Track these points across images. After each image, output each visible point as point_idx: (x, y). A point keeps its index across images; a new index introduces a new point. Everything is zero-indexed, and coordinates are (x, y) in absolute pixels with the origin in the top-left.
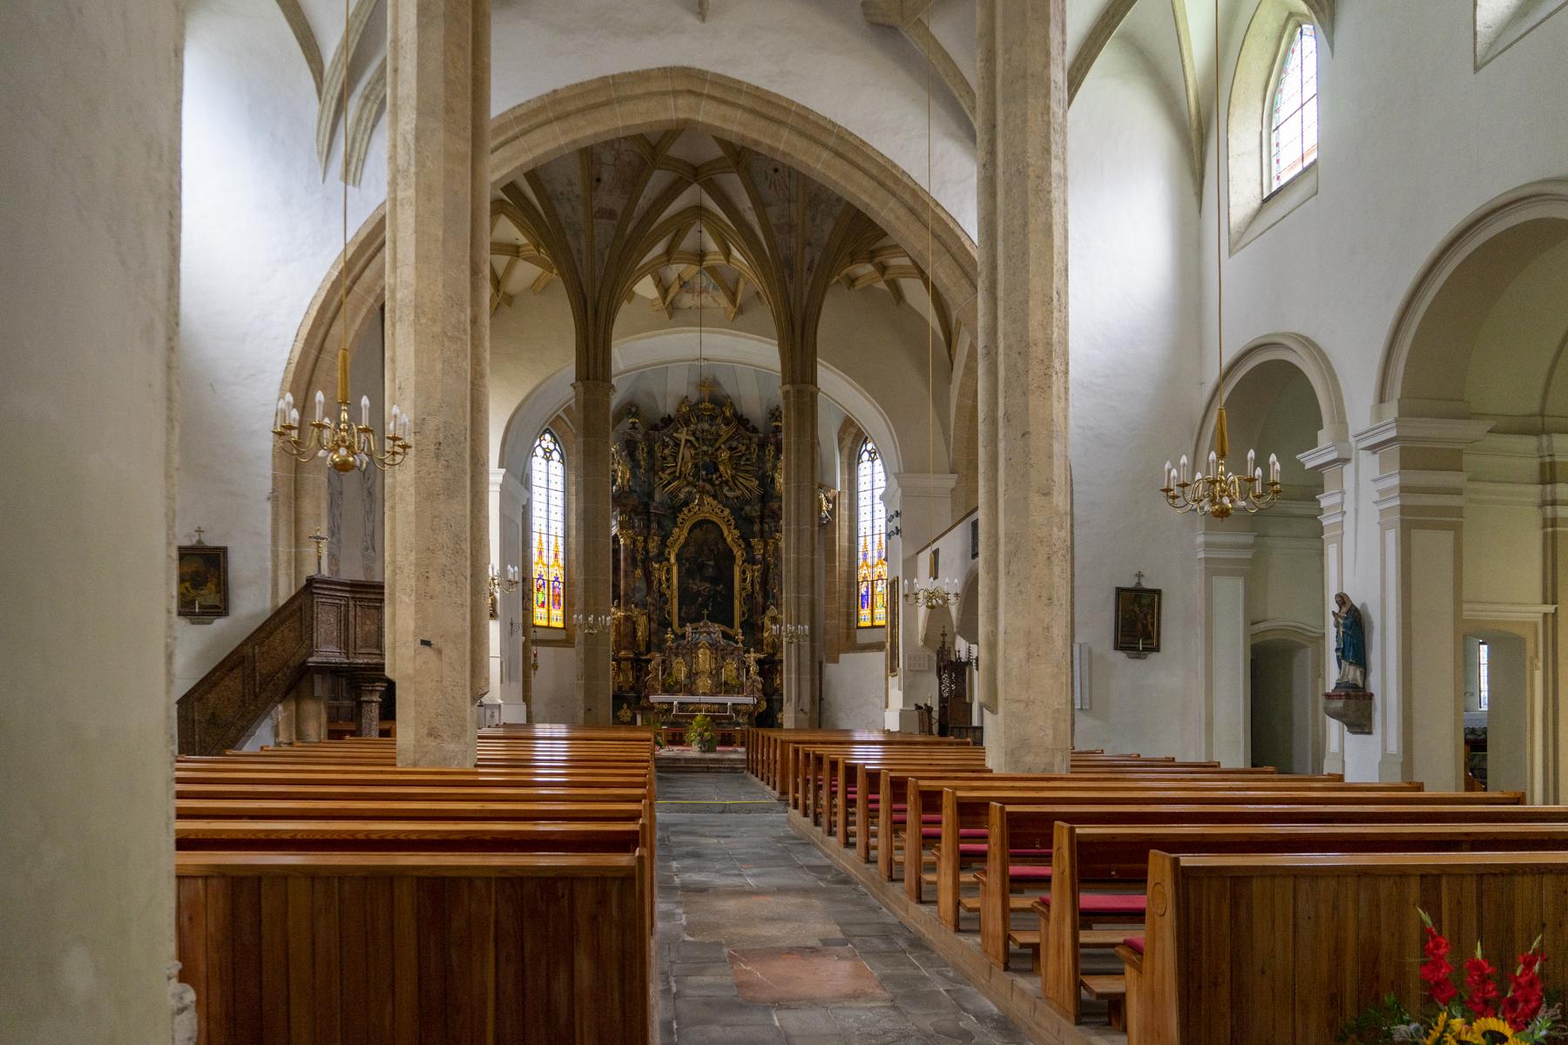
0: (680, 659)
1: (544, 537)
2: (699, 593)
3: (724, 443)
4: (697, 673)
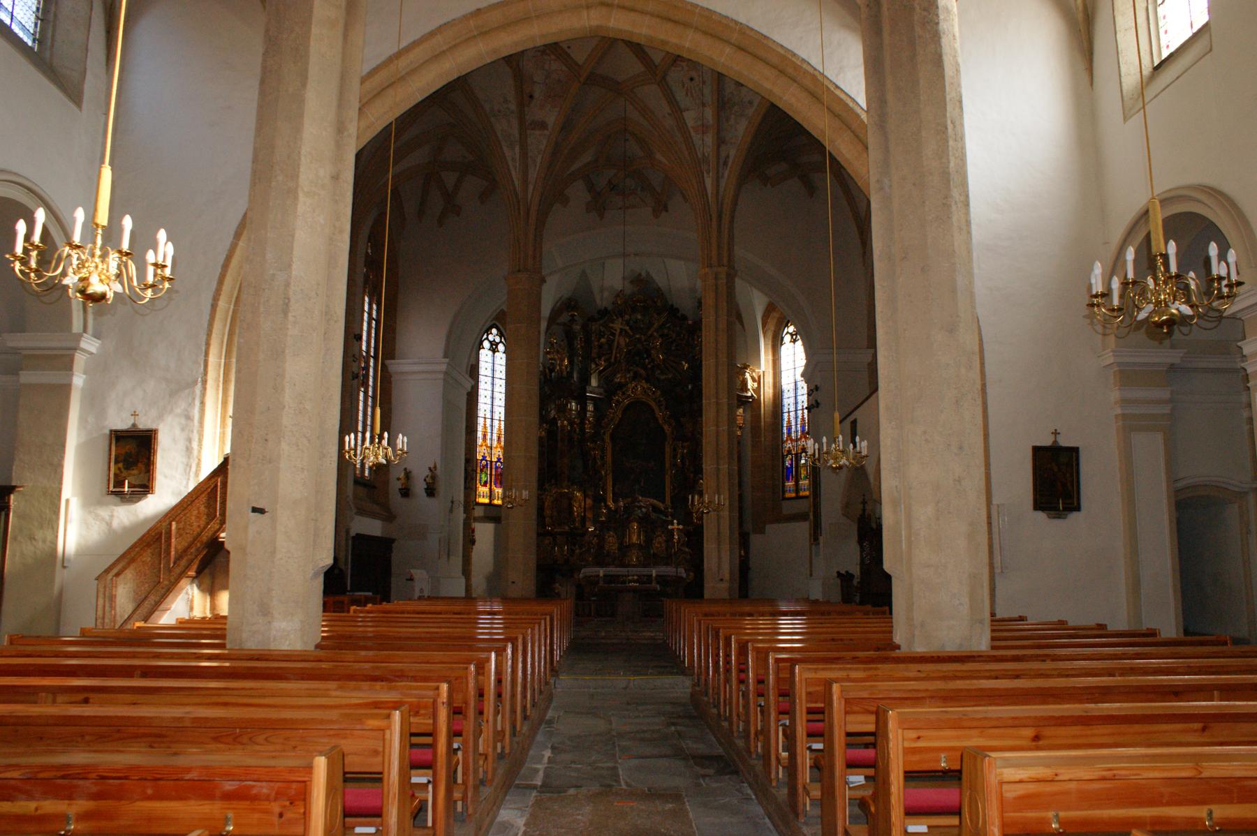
1: (488, 422)
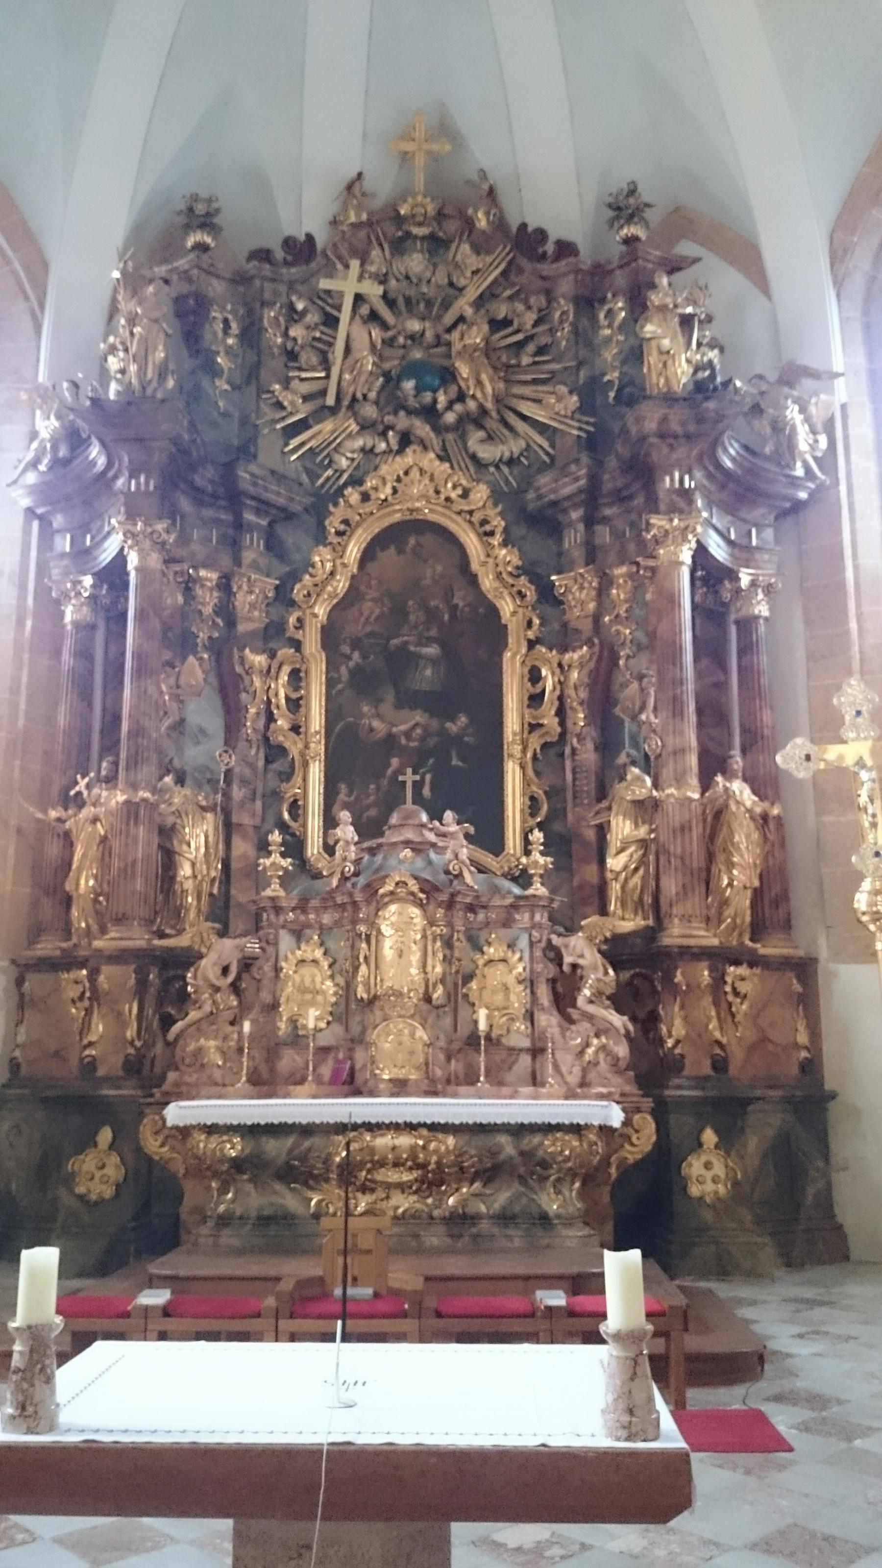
2: (390, 742)
3: (480, 302)
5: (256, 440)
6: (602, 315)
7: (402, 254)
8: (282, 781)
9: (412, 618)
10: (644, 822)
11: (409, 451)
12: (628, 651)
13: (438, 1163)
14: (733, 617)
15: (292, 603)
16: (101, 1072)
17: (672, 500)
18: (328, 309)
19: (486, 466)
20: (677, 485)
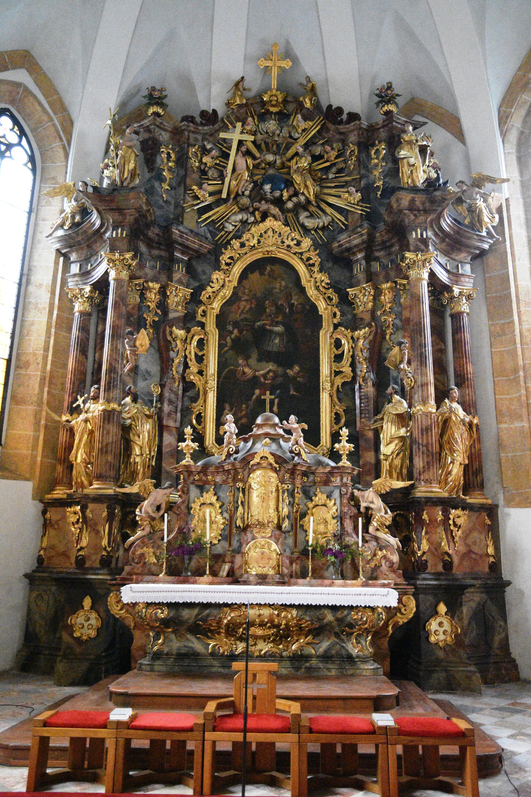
0: (209, 497)
2: (254, 381)
3: (306, 146)
4: (246, 528)
5: (183, 215)
6: (373, 152)
7: (264, 121)
8: (192, 402)
9: (268, 310)
10: (403, 426)
11: (267, 220)
12: (392, 331)
13: (286, 625)
14: (448, 313)
15: (201, 302)
16: (87, 565)
17: (417, 245)
18: (224, 149)
19: (309, 230)
20: (419, 237)
